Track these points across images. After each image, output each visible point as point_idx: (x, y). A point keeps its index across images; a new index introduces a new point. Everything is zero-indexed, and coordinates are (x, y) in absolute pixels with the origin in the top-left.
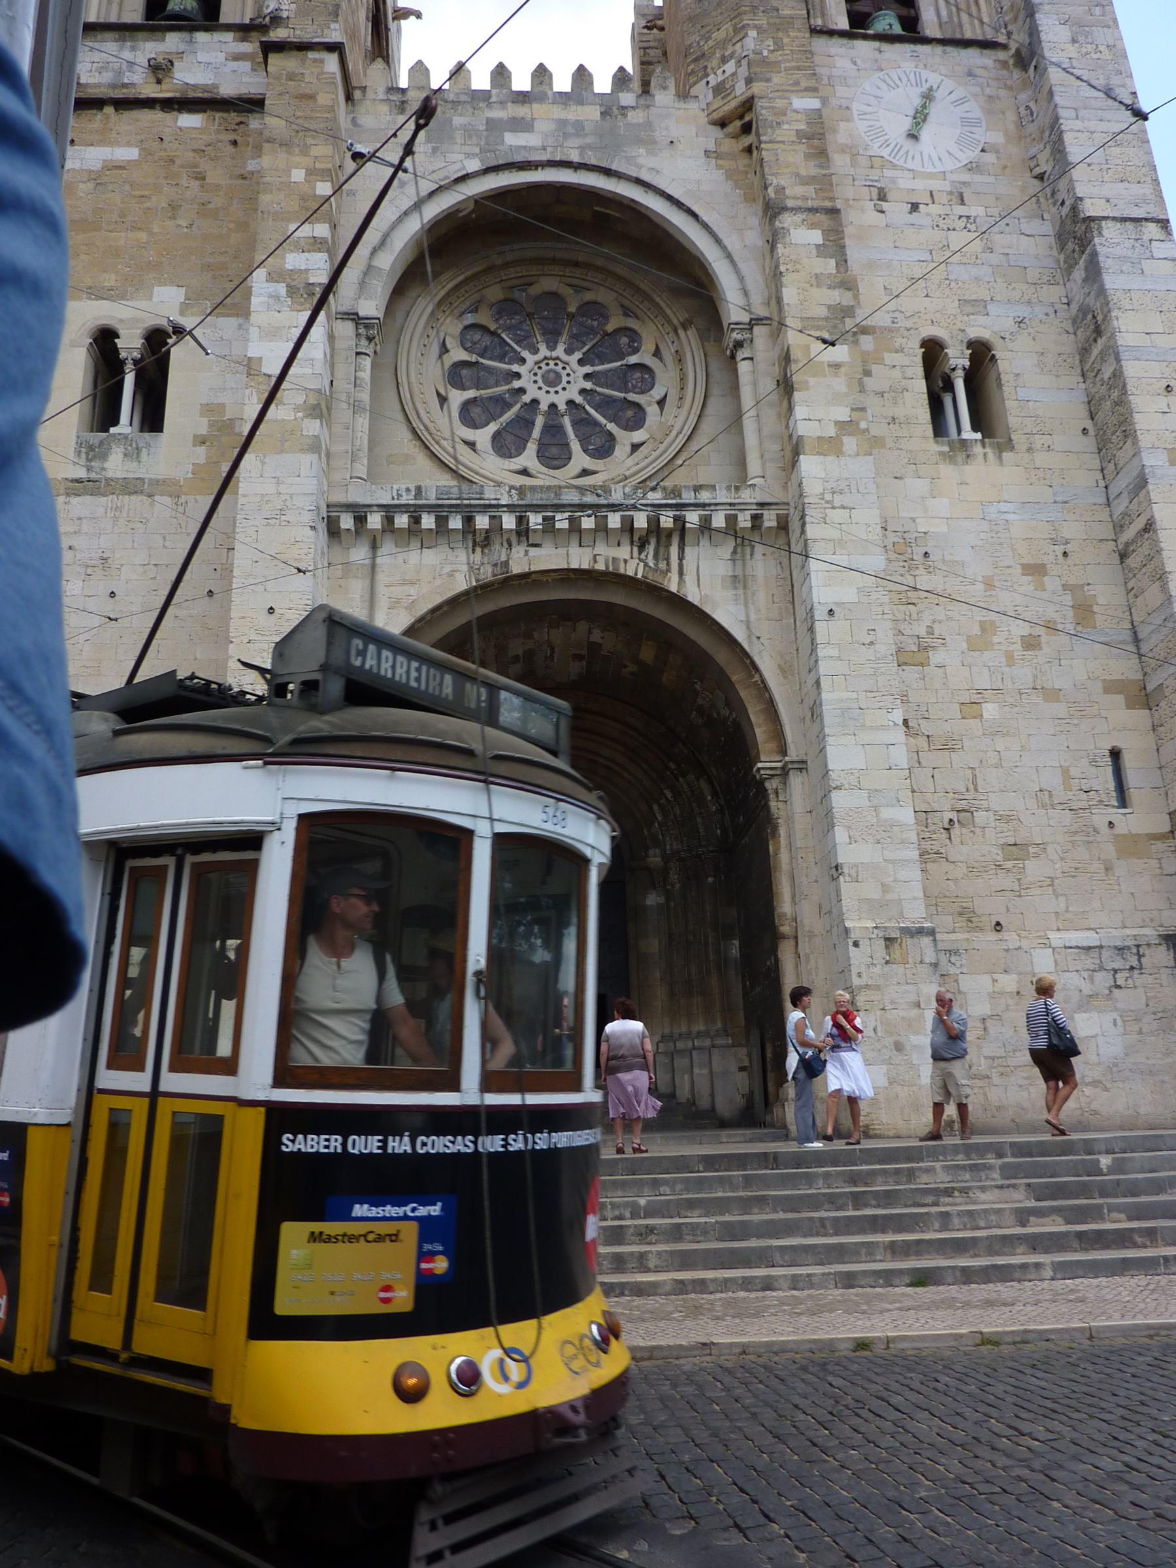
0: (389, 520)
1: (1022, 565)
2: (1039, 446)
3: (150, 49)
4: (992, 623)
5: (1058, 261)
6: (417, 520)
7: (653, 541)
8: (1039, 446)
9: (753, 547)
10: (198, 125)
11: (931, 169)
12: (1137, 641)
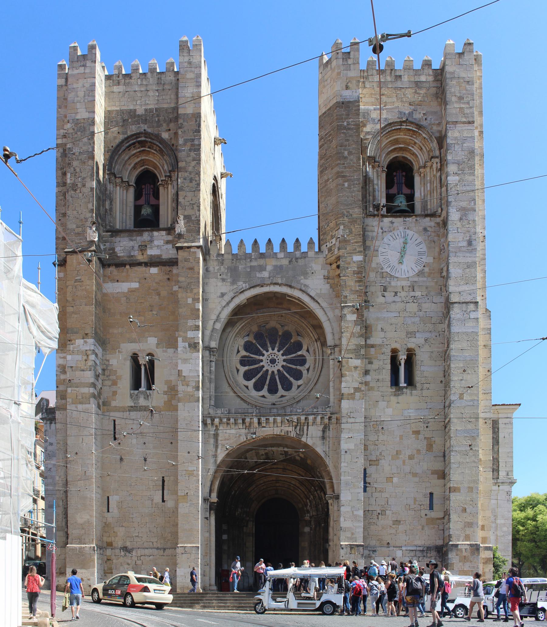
0: (221, 420)
1: (413, 431)
2: (425, 388)
3: (139, 240)
4: (400, 451)
5: (443, 314)
6: (229, 419)
7: (299, 425)
8: (425, 388)
9: (329, 426)
10: (157, 272)
11: (404, 276)
12: (444, 456)
